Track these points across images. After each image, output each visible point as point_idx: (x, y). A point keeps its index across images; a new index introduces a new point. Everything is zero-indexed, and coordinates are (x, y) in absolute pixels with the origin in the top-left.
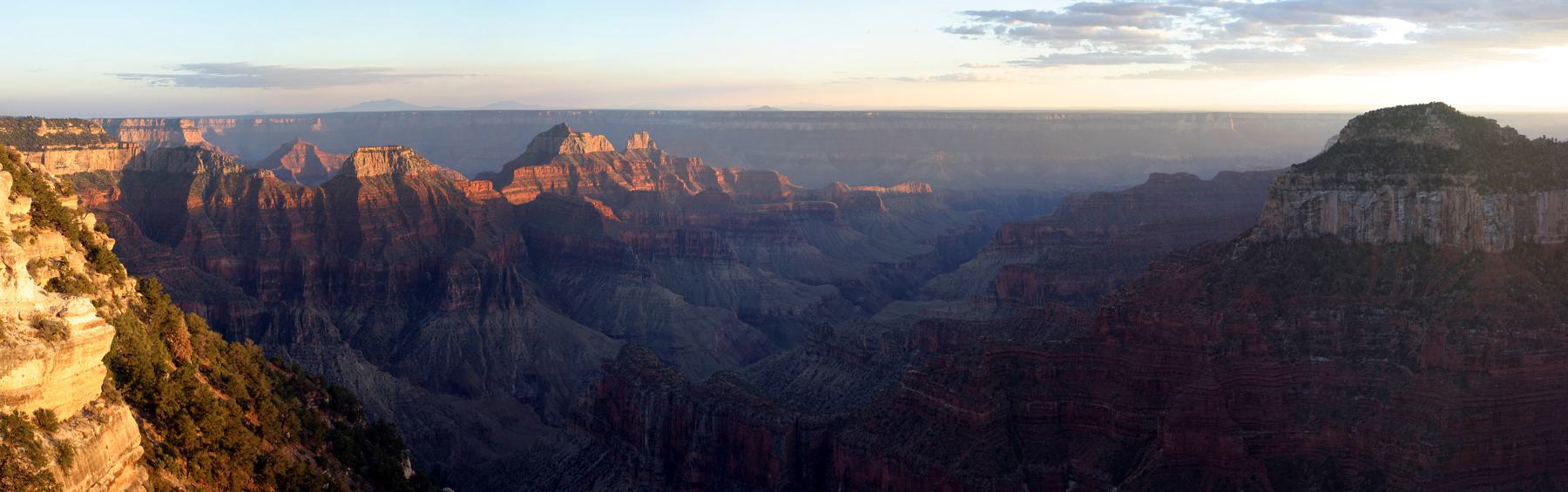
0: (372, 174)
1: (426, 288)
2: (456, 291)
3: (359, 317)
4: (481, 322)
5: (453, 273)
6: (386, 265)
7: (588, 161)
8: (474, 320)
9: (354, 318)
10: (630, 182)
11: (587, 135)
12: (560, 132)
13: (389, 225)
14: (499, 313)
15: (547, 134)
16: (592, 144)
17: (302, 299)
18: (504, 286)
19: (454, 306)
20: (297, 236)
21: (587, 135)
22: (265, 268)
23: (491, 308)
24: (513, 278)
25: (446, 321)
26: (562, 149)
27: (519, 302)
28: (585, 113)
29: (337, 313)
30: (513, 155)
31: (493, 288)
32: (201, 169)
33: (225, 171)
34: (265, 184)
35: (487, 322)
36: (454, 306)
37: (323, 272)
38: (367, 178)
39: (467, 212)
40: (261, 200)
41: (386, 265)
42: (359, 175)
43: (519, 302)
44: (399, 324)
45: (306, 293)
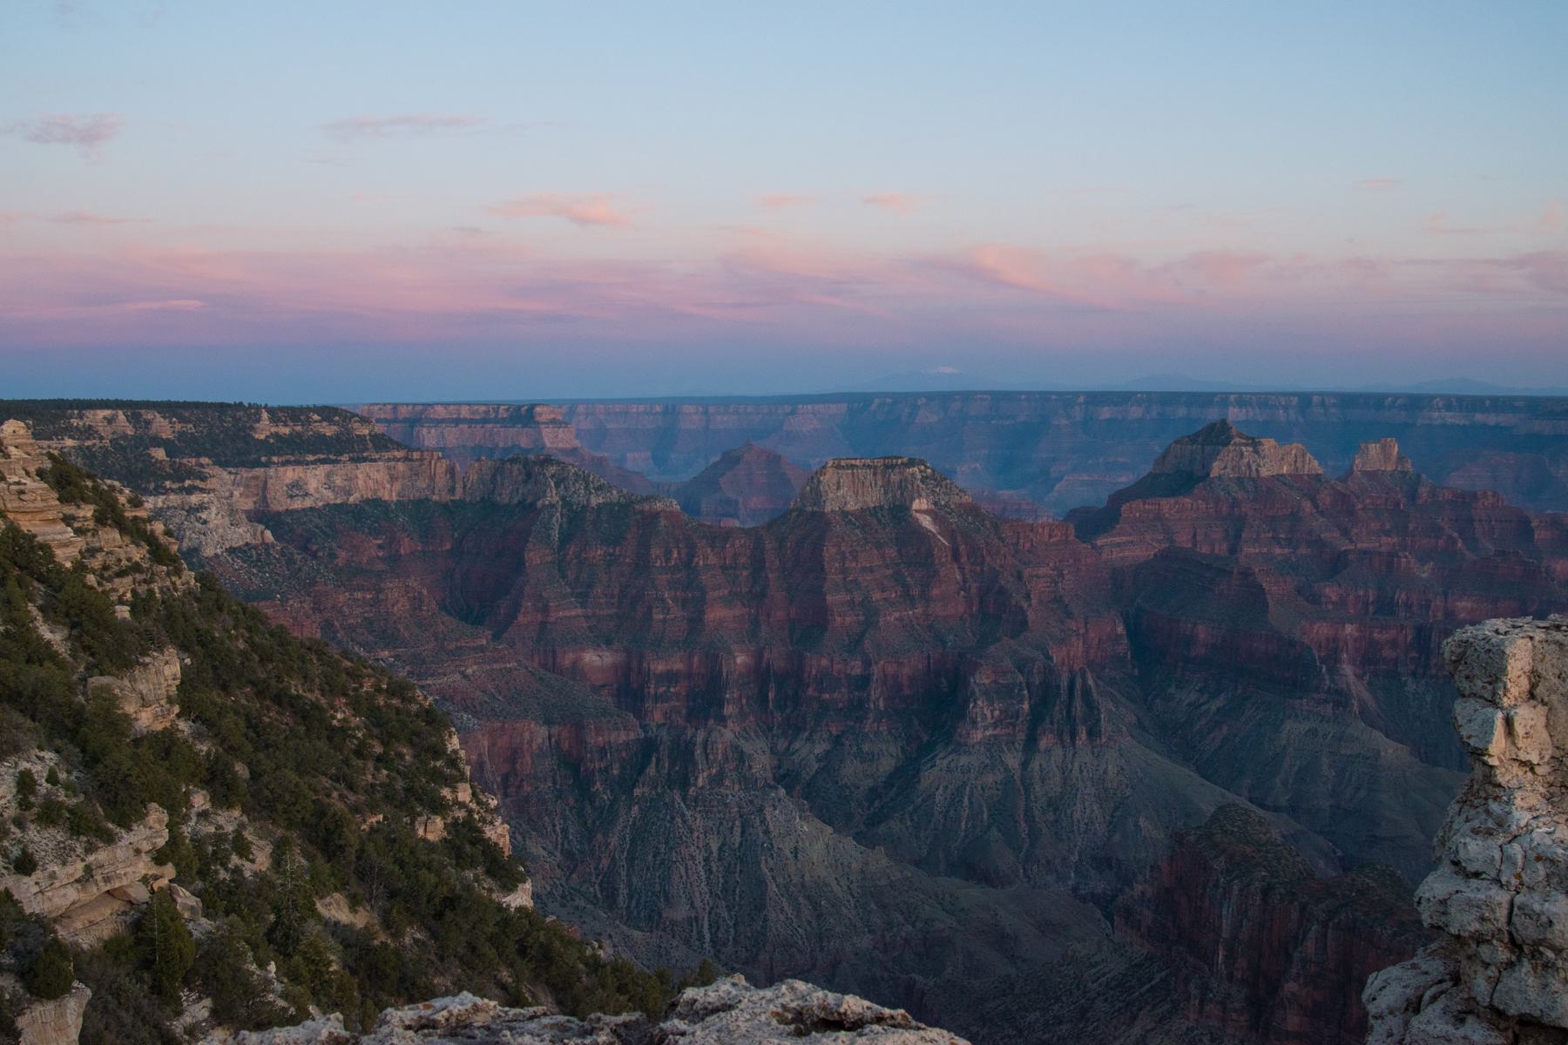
1: (937, 706)
2: (984, 710)
3: (819, 749)
4: (1025, 765)
5: (982, 678)
6: (867, 664)
7: (1265, 491)
8: (1013, 760)
9: (809, 752)
10: (1345, 533)
11: (1268, 444)
12: (1217, 435)
13: (876, 596)
14: (1058, 752)
15: (1193, 439)
16: (1275, 460)
17: (722, 720)
18: (1069, 707)
19: (978, 736)
20: (716, 614)
22: (660, 667)
23: (1043, 743)
24: (1086, 692)
25: (964, 760)
26: (1216, 469)
27: (1093, 734)
28: (1264, 400)
29: (782, 745)
30: (1125, 480)
31: (1050, 706)
32: (552, 496)
33: (595, 501)
34: (663, 522)
35: (1035, 765)
36: (978, 736)
37: (761, 674)
38: (845, 514)
39: (1020, 577)
40: (656, 551)
41: (867, 664)
42: (828, 509)
43: (1093, 734)
44: (887, 765)
45: (729, 710)
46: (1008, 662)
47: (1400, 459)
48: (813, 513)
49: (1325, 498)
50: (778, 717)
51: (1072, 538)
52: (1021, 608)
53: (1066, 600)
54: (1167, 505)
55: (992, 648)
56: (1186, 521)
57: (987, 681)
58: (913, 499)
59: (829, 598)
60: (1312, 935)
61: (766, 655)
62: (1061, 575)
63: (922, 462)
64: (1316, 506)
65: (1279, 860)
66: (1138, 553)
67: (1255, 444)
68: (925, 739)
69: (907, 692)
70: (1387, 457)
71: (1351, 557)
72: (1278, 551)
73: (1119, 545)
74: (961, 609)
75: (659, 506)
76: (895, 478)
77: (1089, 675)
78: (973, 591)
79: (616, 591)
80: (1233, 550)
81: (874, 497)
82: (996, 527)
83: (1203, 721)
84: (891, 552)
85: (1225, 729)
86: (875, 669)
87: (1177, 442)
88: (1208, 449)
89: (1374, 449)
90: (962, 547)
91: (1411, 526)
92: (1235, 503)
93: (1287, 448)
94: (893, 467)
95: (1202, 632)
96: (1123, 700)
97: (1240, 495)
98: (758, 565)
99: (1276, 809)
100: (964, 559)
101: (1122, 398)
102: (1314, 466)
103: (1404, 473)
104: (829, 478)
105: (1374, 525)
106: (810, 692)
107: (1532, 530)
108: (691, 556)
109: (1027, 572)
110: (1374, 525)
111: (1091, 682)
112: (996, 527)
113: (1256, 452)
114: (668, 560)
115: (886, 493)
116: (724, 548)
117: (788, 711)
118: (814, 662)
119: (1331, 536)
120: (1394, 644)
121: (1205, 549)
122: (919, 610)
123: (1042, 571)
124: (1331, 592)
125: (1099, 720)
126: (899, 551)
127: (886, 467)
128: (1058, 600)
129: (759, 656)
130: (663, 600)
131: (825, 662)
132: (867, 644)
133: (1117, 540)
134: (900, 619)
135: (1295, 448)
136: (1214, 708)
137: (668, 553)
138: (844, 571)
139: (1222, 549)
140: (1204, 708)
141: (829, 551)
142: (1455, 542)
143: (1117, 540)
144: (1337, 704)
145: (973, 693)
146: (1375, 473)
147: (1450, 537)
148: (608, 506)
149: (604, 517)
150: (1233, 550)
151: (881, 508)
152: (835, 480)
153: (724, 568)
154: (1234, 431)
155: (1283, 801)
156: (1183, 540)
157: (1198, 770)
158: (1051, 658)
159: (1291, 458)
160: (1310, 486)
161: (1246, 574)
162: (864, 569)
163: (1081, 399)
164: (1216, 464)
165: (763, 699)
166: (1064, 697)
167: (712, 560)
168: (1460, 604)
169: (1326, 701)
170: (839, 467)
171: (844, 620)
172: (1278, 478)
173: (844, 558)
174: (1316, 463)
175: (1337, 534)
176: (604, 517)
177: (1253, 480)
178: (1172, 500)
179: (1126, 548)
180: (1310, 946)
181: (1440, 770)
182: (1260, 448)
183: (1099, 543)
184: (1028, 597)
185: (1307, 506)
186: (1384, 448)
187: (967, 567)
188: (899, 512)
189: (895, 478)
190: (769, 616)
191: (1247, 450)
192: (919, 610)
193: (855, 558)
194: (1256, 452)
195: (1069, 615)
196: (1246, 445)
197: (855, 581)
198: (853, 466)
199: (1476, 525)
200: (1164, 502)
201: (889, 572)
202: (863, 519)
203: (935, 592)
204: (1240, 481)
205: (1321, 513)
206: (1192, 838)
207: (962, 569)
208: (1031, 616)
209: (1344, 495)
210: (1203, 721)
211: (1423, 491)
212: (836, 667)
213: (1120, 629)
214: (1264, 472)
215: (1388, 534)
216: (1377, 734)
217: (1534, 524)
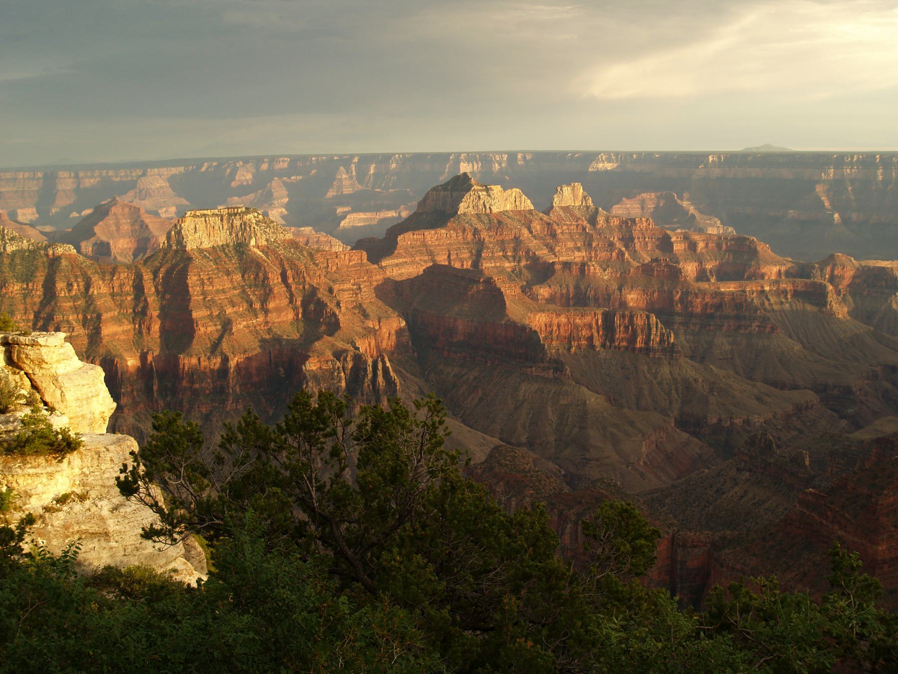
0: (206, 245)
6: (225, 360)
7: (497, 223)
10: (552, 250)
11: (497, 189)
12: (461, 184)
13: (229, 310)
15: (445, 187)
16: (504, 201)
20: (108, 330)
21: (497, 189)
24: (386, 371)
26: (462, 208)
33: (10, 249)
34: (64, 263)
38: (201, 251)
39: (331, 290)
40: (60, 285)
42: (188, 248)
46: (329, 354)
47: (584, 197)
48: (176, 251)
49: (537, 226)
50: (161, 403)
51: (365, 261)
52: (334, 314)
53: (364, 306)
54: (430, 236)
55: (316, 344)
56: (443, 246)
57: (314, 368)
58: (250, 238)
59: (195, 315)
60: (568, 530)
61: (150, 358)
62: (360, 289)
63: (255, 211)
64: (531, 232)
65: (540, 481)
66: (411, 270)
68: (271, 412)
69: (255, 379)
70: (575, 197)
71: (557, 267)
72: (507, 265)
73: (397, 265)
74: (291, 316)
75: (60, 250)
76: (237, 222)
77: (386, 359)
78: (299, 303)
79: (32, 317)
80: (476, 264)
81: (222, 237)
82: (311, 255)
83: (465, 388)
84: (238, 277)
85: (480, 392)
86: (233, 363)
87: (435, 189)
88: (455, 194)
89: (567, 190)
90: (289, 273)
91: (594, 245)
92: (476, 232)
94: (235, 215)
95: (460, 325)
96: (408, 375)
97: (479, 226)
98: (139, 288)
99: (520, 445)
100: (290, 281)
102: (527, 204)
103: (588, 207)
104: (188, 225)
105: (570, 244)
106: (184, 383)
107: (672, 245)
108: (88, 286)
109: (336, 287)
110: (570, 244)
111: (388, 364)
112: (311, 255)
113: (489, 195)
114: (70, 291)
115: (231, 234)
116: (112, 279)
117: (169, 399)
118: (186, 361)
119: (543, 253)
120: (590, 327)
121: (457, 265)
122: (261, 319)
123: (347, 286)
124: (544, 292)
125: (395, 391)
126: (243, 276)
127: (230, 215)
128: (360, 306)
129: (143, 357)
130: (68, 321)
131: (194, 361)
132: (225, 345)
133: (396, 261)
134: (248, 327)
135: (516, 191)
136: (471, 378)
137: (70, 285)
138: (204, 293)
139: (468, 265)
140: (465, 378)
141: (192, 279)
142: (623, 254)
143: (396, 261)
144: (556, 370)
145: (305, 377)
146: (568, 207)
147: (620, 251)
148: (21, 251)
149: (18, 261)
150: (476, 264)
151: (228, 245)
152: (193, 226)
153: (113, 295)
154: (473, 181)
155: (524, 439)
156: (442, 259)
157: (464, 422)
158: (358, 349)
160: (526, 219)
161: (489, 281)
162: (217, 292)
163: (356, 160)
164: (461, 205)
165: (149, 390)
166: (370, 376)
167: (104, 290)
168: (630, 297)
169: (549, 368)
170: (195, 216)
171: (206, 329)
172: (504, 213)
173: (203, 284)
175: (546, 251)
176: (18, 261)
177: (488, 215)
178: (433, 232)
179: (403, 267)
180: (567, 538)
181: (626, 410)
182: (491, 192)
183: (384, 264)
184: (338, 304)
185: (525, 232)
186: (573, 190)
187: (293, 287)
188: (241, 248)
189: (237, 222)
190: (149, 329)
191: (483, 194)
192: (261, 319)
193: (211, 283)
194: (489, 195)
195: (366, 316)
197: (212, 299)
198: (205, 215)
199: (636, 241)
201: (238, 291)
202: (216, 253)
203: (271, 305)
204: (478, 216)
205: (534, 237)
206: (479, 471)
207: (288, 286)
208: (341, 318)
209: (548, 224)
210: (465, 388)
211: (601, 220)
212: (203, 364)
213: (403, 324)
214: (495, 210)
215: (579, 249)
216: (585, 389)
217: (673, 239)
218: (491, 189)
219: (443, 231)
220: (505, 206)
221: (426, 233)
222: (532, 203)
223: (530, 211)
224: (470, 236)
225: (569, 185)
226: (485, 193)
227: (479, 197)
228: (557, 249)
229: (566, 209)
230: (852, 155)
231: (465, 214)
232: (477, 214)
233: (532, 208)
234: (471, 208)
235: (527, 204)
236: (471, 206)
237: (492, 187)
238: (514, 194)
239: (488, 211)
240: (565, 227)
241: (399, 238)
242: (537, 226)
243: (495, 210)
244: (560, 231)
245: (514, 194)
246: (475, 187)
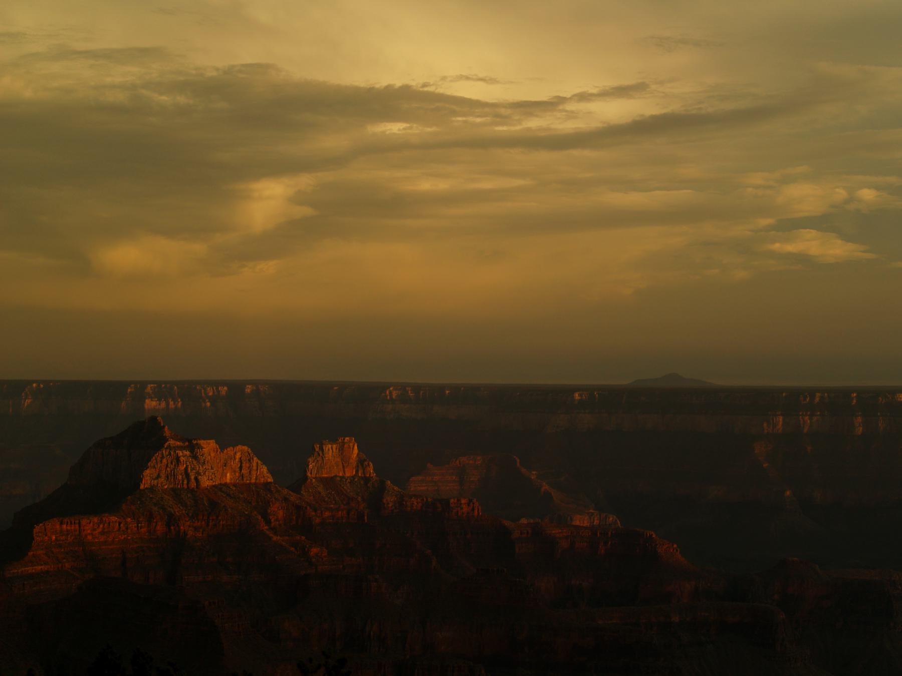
11: (208, 447)
12: (145, 437)
16: (220, 466)
21: (208, 447)
26: (148, 478)
47: (361, 462)
67: (193, 448)
89: (330, 450)
93: (230, 451)
101: (791, 401)
102: (262, 473)
103: (367, 480)
113: (195, 457)
135: (240, 451)
154: (167, 432)
159: (235, 464)
164: (147, 472)
174: (265, 469)
177: (193, 490)
178: (96, 520)
186: (341, 449)
191: (184, 454)
194: (195, 457)
196: (182, 448)
200: (84, 522)
211: (389, 500)
214: (205, 482)
218: (200, 447)
219: (114, 519)
220: (224, 475)
221: (84, 522)
222: (270, 471)
223: (267, 484)
224: (160, 528)
225: (334, 441)
226: (188, 453)
227: (178, 459)
228: (314, 550)
229: (329, 482)
230: (812, 392)
231: (152, 489)
232: (173, 490)
233: (270, 480)
234: (162, 480)
235: (262, 473)
236: (163, 475)
237: (202, 442)
238: (238, 456)
239: (193, 484)
240: (327, 514)
241: (37, 529)
242: (278, 512)
243: (205, 482)
244: (318, 520)
245: (238, 456)
246: (172, 442)
